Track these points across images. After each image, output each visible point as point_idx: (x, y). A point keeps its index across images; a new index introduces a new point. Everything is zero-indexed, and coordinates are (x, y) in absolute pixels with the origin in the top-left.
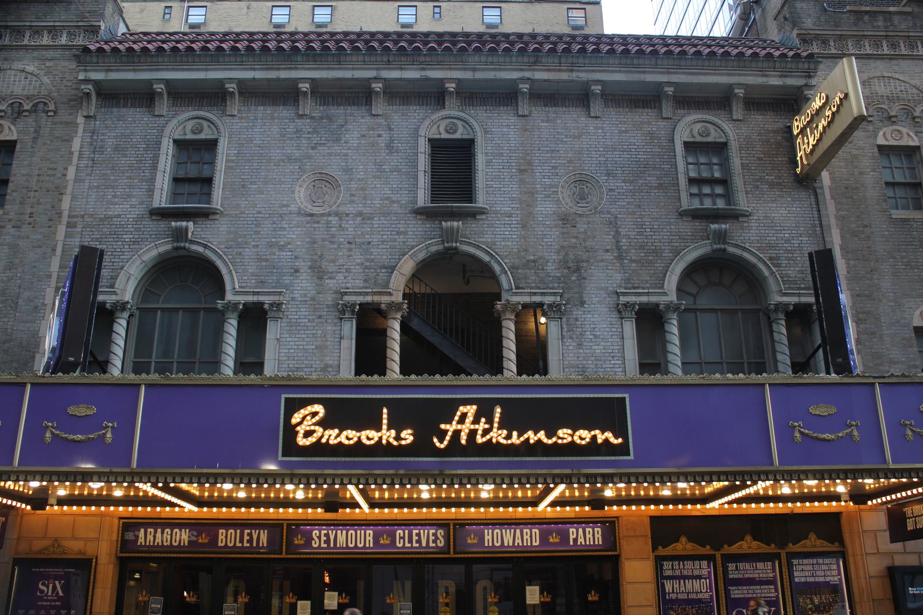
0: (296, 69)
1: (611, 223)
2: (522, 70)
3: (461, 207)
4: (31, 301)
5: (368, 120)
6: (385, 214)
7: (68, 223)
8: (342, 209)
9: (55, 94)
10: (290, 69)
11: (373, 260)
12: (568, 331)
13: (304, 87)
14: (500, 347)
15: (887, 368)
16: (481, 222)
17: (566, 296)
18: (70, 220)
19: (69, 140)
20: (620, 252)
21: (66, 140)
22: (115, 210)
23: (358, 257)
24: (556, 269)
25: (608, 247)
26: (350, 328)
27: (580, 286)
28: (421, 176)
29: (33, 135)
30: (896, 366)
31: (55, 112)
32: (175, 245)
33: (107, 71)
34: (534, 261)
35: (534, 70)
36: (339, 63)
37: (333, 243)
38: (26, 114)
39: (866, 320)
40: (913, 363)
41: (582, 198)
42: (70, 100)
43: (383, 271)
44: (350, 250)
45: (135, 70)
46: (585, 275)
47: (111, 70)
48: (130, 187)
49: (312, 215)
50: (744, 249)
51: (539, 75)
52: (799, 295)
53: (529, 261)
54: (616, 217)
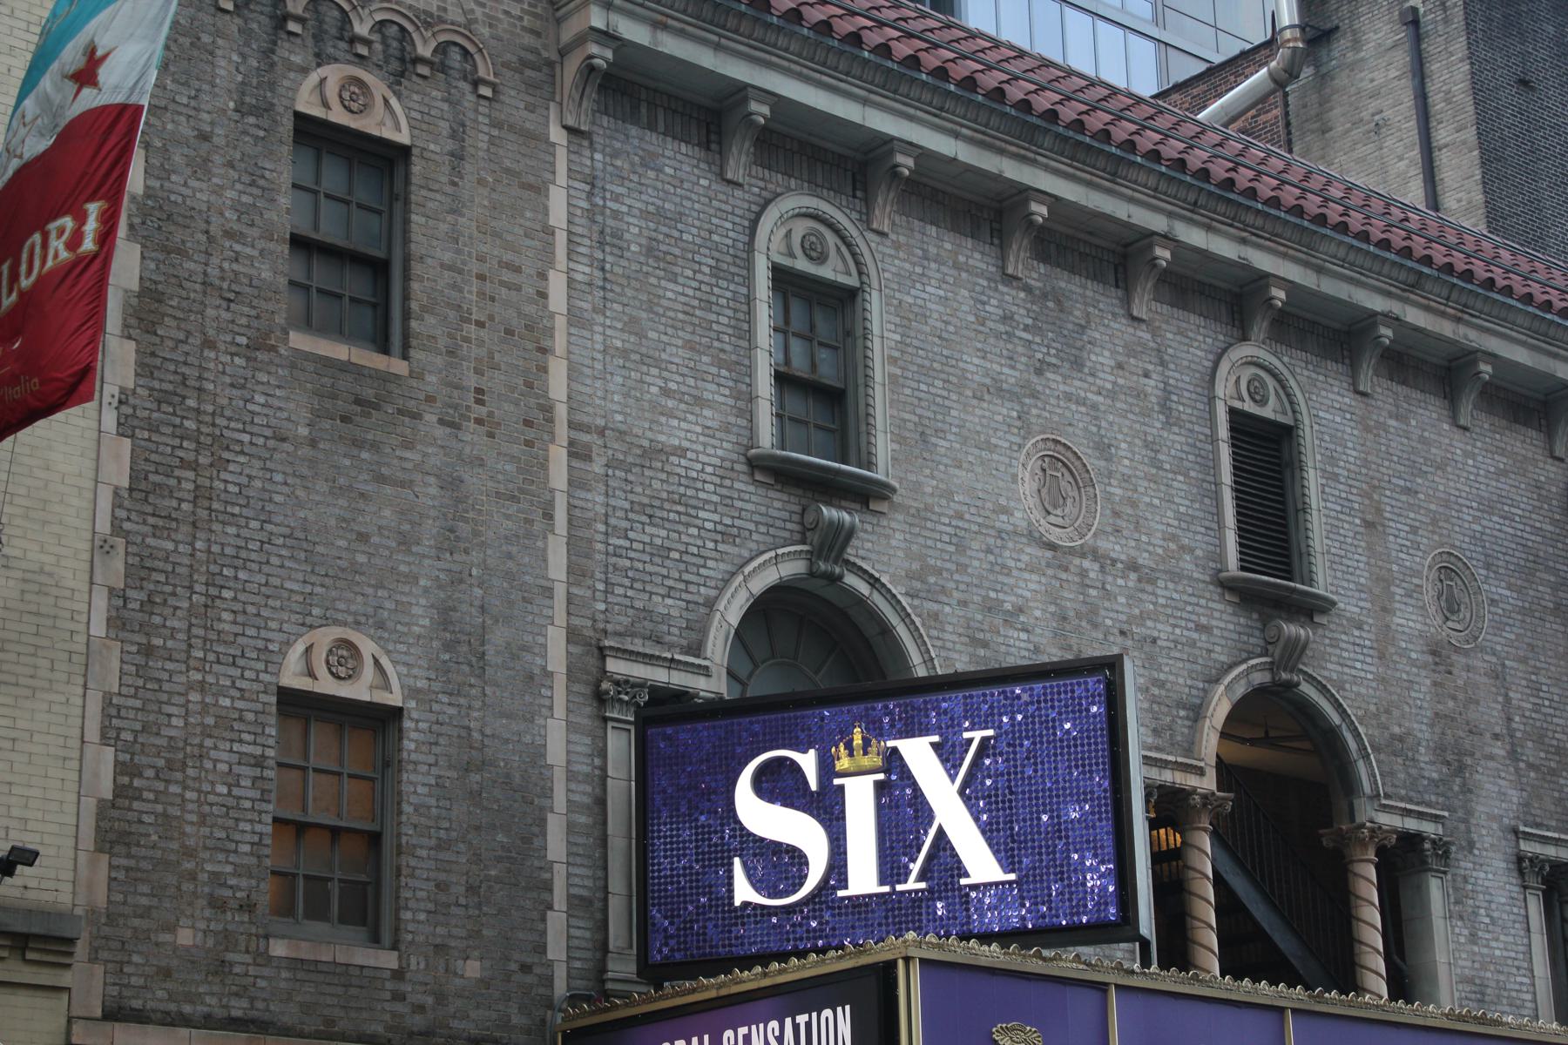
0: (1033, 163)
2: (1389, 294)
4: (514, 657)
5: (1120, 325)
6: (1176, 577)
7: (571, 443)
8: (1104, 545)
9: (486, 31)
10: (1023, 159)
12: (1457, 902)
13: (1040, 210)
16: (1320, 631)
18: (574, 434)
19: (539, 190)
20: (1513, 744)
21: (530, 187)
22: (674, 433)
25: (1497, 730)
29: (450, 145)
31: (493, 86)
32: (823, 566)
33: (657, 25)
34: (1401, 739)
35: (1406, 301)
36: (1114, 176)
37: (1095, 626)
38: (423, 70)
41: (1453, 612)
42: (524, 63)
43: (1182, 713)
45: (717, 47)
47: (665, 27)
48: (698, 375)
49: (1052, 547)
51: (1415, 316)
53: (1393, 737)
54: (1503, 665)
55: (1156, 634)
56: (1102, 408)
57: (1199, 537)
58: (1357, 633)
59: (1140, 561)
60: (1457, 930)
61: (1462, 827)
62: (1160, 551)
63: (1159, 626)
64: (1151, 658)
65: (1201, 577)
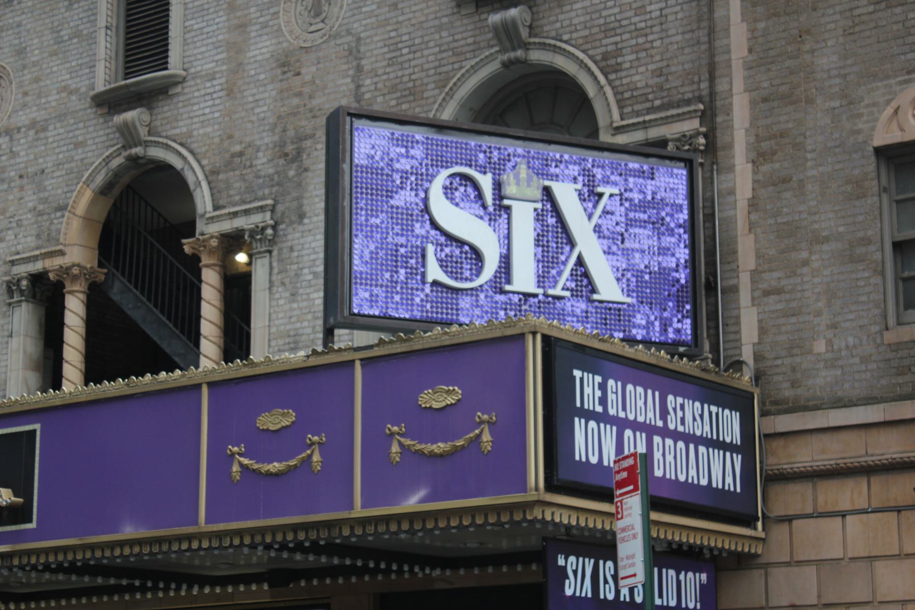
1: (351, 53)
3: (138, 83)
6: (61, 117)
11: (47, 199)
12: (280, 272)
14: (196, 317)
15: (804, 255)
16: (175, 100)
17: (280, 208)
23: (31, 200)
24: (270, 161)
26: (23, 319)
27: (299, 184)
28: (101, 36)
30: (825, 247)
34: (241, 154)
39: (774, 153)
40: (861, 234)
43: (59, 214)
44: (22, 188)
46: (307, 163)
50: (556, 49)
52: (645, 125)
53: (233, 156)
54: (359, 39)
55: (45, 165)
56: (24, 22)
57: (84, 77)
58: (208, 84)
59: (38, 119)
60: (277, 296)
61: (295, 203)
62: (54, 104)
63: (48, 159)
64: (41, 188)
65: (83, 107)
